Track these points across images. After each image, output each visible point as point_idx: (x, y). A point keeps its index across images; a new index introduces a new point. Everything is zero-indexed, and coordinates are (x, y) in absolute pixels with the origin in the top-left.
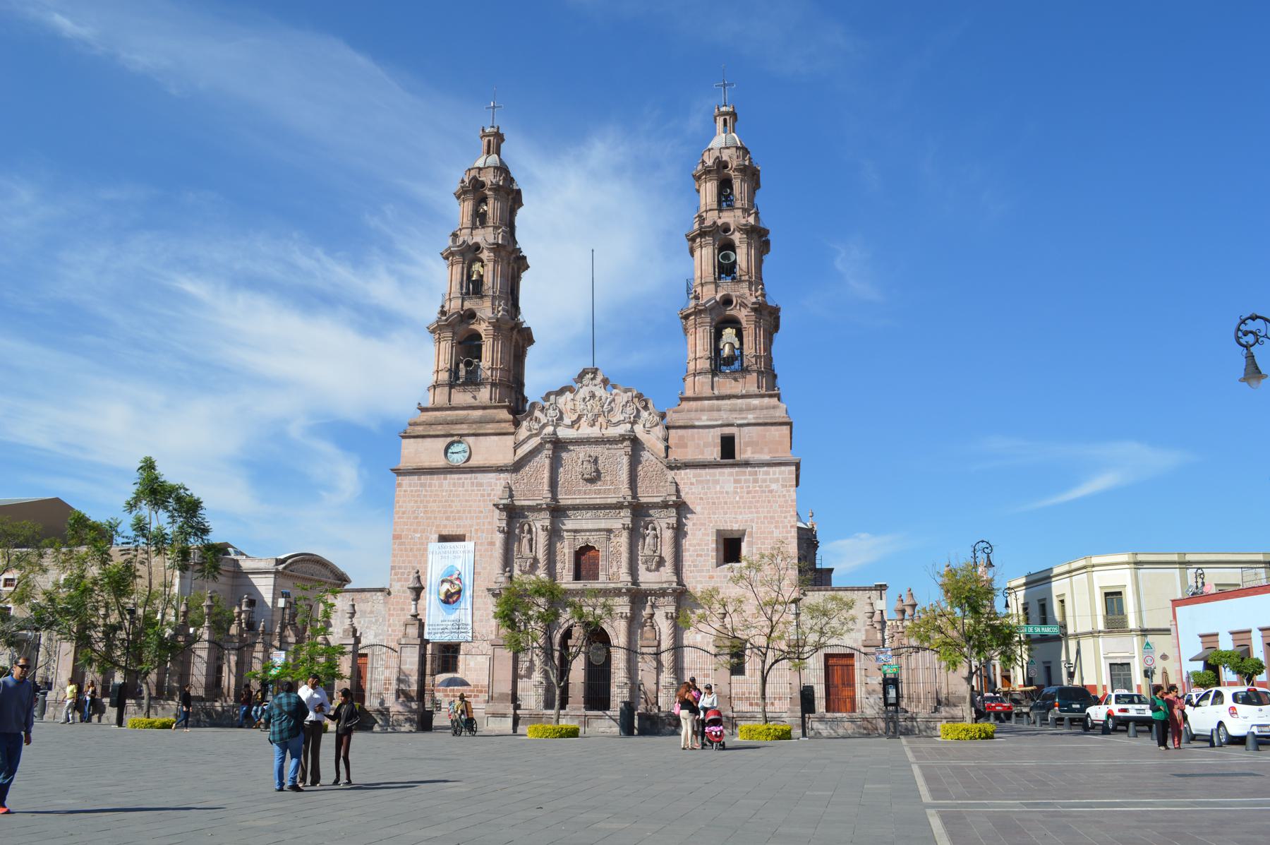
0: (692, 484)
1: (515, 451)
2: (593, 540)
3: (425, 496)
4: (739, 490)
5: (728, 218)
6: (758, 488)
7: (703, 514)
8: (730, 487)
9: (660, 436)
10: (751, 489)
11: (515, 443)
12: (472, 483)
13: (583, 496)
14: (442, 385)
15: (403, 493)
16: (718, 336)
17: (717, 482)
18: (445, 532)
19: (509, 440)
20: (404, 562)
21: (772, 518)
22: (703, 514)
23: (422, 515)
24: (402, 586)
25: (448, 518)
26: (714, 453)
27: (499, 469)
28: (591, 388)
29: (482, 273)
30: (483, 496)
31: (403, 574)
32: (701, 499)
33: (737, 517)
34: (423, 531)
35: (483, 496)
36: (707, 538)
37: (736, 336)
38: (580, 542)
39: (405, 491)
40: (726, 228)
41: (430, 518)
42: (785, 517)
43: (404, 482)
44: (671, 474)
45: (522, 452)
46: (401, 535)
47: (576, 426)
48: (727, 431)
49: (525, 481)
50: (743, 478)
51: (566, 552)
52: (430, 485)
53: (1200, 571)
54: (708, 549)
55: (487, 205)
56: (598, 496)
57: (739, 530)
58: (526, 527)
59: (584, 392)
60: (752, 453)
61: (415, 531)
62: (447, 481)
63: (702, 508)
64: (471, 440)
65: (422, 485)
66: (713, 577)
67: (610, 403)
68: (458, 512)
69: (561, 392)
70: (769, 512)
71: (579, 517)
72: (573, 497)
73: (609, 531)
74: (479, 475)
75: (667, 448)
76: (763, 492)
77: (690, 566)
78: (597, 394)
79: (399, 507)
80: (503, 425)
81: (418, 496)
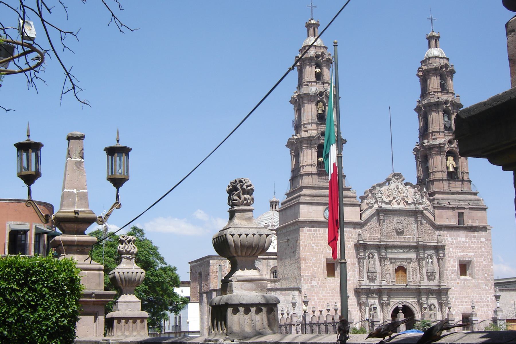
0: (447, 237)
1: (361, 215)
2: (404, 264)
3: (317, 237)
4: (468, 241)
5: (443, 97)
6: (476, 240)
7: (453, 251)
8: (464, 239)
10: (473, 240)
11: (361, 211)
13: (397, 241)
14: (314, 174)
15: (304, 235)
16: (447, 160)
17: (458, 236)
19: (358, 209)
20: (308, 273)
22: (453, 251)
24: (308, 286)
26: (454, 222)
28: (397, 183)
31: (308, 280)
32: (452, 244)
33: (467, 253)
34: (317, 256)
36: (455, 264)
37: (454, 160)
38: (398, 264)
39: (305, 233)
40: (446, 102)
41: (320, 249)
44: (437, 233)
45: (365, 216)
46: (305, 258)
47: (391, 204)
48: (460, 211)
49: (368, 231)
51: (391, 267)
54: (456, 269)
56: (405, 241)
57: (469, 260)
58: (371, 255)
59: (393, 185)
60: (472, 223)
61: (313, 256)
63: (452, 249)
66: (459, 284)
67: (407, 192)
69: (380, 185)
70: (481, 252)
71: (396, 252)
72: (393, 241)
73: (410, 259)
75: (434, 217)
76: (478, 242)
77: (448, 277)
79: (303, 243)
80: (352, 200)
81: (313, 237)
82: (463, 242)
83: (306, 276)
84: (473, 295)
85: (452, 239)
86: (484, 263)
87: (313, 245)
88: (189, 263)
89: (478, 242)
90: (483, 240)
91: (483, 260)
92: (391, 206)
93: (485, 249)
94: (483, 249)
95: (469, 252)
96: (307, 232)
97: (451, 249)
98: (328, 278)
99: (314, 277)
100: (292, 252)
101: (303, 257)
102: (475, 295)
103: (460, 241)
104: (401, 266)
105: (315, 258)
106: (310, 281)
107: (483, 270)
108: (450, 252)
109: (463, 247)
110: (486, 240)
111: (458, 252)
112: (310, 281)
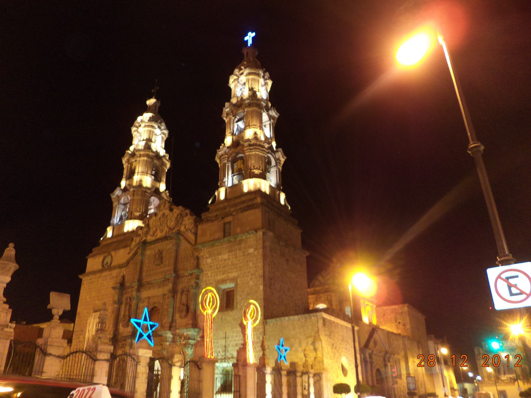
7: (211, 276)
8: (226, 257)
9: (193, 231)
17: (220, 254)
18: (96, 309)
21: (249, 272)
25: (98, 300)
27: (120, 267)
32: (211, 267)
42: (256, 271)
47: (155, 235)
63: (211, 273)
64: (113, 253)
75: (196, 238)
78: (166, 214)
82: (225, 260)
84: (231, 334)
85: (212, 260)
86: (251, 283)
87: (87, 297)
89: (244, 255)
90: (251, 251)
91: (249, 280)
92: (156, 237)
93: (253, 264)
94: (251, 264)
95: (231, 272)
97: (209, 274)
102: (235, 334)
103: (221, 260)
108: (208, 277)
109: (224, 267)
110: (254, 250)
111: (217, 275)
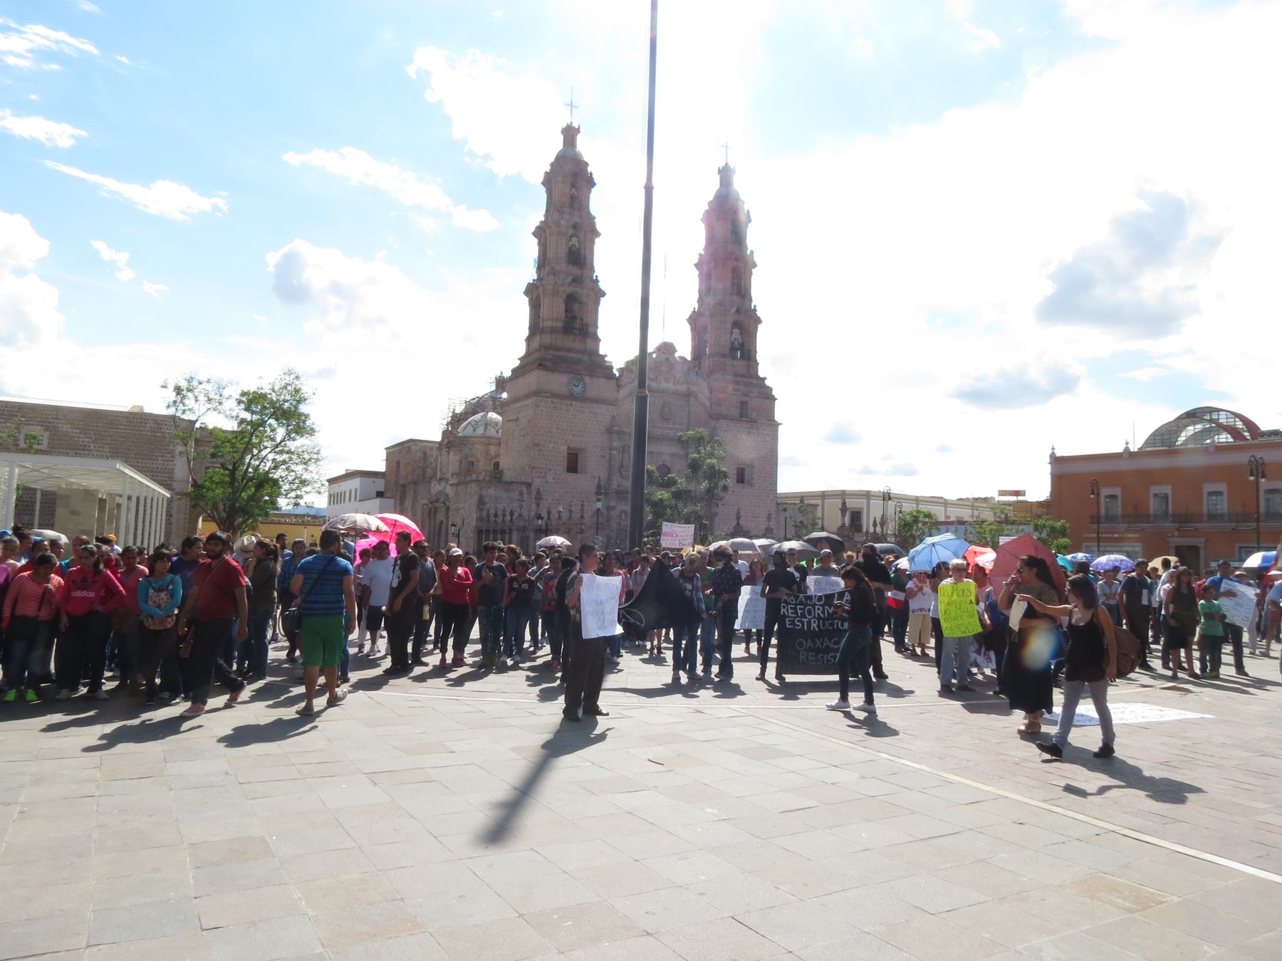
3: (557, 416)
12: (590, 412)
18: (572, 445)
23: (555, 430)
25: (573, 435)
26: (735, 412)
29: (577, 247)
30: (597, 421)
31: (541, 473)
35: (597, 421)
43: (541, 404)
48: (744, 399)
50: (752, 431)
52: (561, 409)
53: (899, 504)
55: (577, 190)
58: (626, 447)
61: (550, 442)
62: (572, 408)
64: (587, 379)
65: (555, 408)
68: (581, 432)
74: (595, 405)
83: (540, 468)
88: (386, 449)
96: (544, 409)
98: (568, 474)
99: (550, 470)
100: (522, 435)
101: (537, 442)
104: (664, 464)
105: (552, 445)
106: (543, 474)
107: (765, 477)
112: (543, 474)
